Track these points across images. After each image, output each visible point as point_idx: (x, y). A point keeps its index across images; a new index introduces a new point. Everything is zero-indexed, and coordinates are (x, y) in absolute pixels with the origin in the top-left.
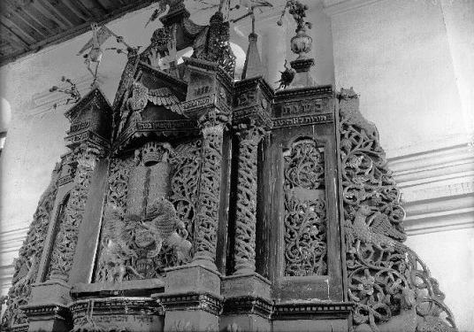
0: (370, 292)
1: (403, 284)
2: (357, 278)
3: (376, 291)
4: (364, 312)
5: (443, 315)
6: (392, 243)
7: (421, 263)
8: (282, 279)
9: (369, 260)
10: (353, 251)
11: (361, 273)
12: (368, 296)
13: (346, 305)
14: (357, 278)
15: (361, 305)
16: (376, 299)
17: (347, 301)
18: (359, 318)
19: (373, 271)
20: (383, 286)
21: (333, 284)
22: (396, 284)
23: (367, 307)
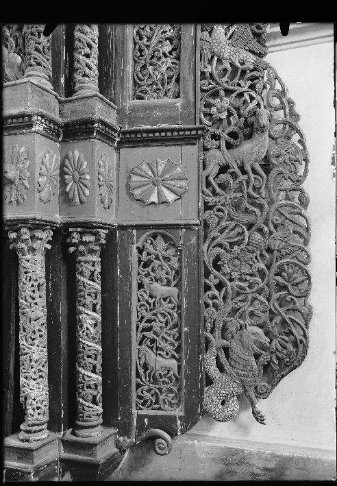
0: (224, 115)
1: (258, 105)
2: (211, 100)
3: (230, 114)
4: (215, 137)
5: (296, 137)
6: (251, 58)
7: (280, 82)
8: (130, 103)
9: (225, 79)
10: (209, 69)
11: (215, 94)
12: (221, 120)
13: (197, 129)
14: (211, 100)
15: (212, 130)
16: (229, 123)
17: (198, 125)
18: (211, 144)
19: (228, 92)
20: (237, 109)
21: (184, 107)
22: (252, 106)
23: (218, 132)
